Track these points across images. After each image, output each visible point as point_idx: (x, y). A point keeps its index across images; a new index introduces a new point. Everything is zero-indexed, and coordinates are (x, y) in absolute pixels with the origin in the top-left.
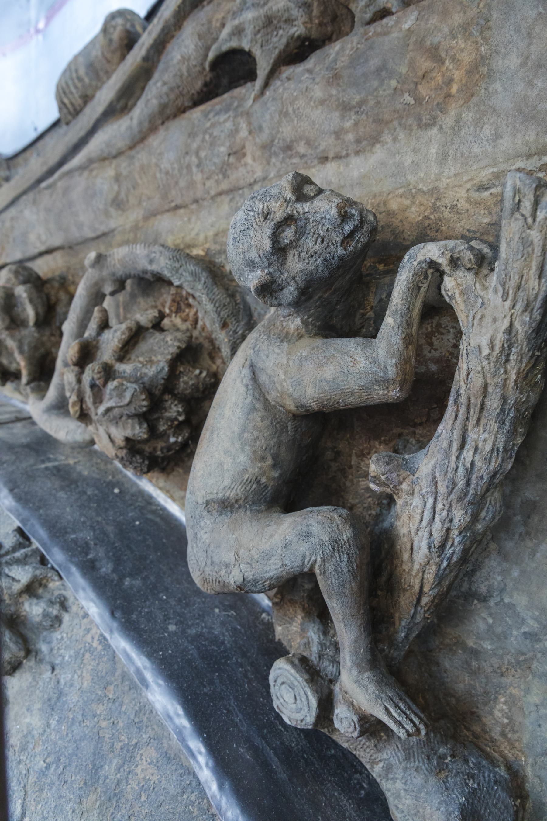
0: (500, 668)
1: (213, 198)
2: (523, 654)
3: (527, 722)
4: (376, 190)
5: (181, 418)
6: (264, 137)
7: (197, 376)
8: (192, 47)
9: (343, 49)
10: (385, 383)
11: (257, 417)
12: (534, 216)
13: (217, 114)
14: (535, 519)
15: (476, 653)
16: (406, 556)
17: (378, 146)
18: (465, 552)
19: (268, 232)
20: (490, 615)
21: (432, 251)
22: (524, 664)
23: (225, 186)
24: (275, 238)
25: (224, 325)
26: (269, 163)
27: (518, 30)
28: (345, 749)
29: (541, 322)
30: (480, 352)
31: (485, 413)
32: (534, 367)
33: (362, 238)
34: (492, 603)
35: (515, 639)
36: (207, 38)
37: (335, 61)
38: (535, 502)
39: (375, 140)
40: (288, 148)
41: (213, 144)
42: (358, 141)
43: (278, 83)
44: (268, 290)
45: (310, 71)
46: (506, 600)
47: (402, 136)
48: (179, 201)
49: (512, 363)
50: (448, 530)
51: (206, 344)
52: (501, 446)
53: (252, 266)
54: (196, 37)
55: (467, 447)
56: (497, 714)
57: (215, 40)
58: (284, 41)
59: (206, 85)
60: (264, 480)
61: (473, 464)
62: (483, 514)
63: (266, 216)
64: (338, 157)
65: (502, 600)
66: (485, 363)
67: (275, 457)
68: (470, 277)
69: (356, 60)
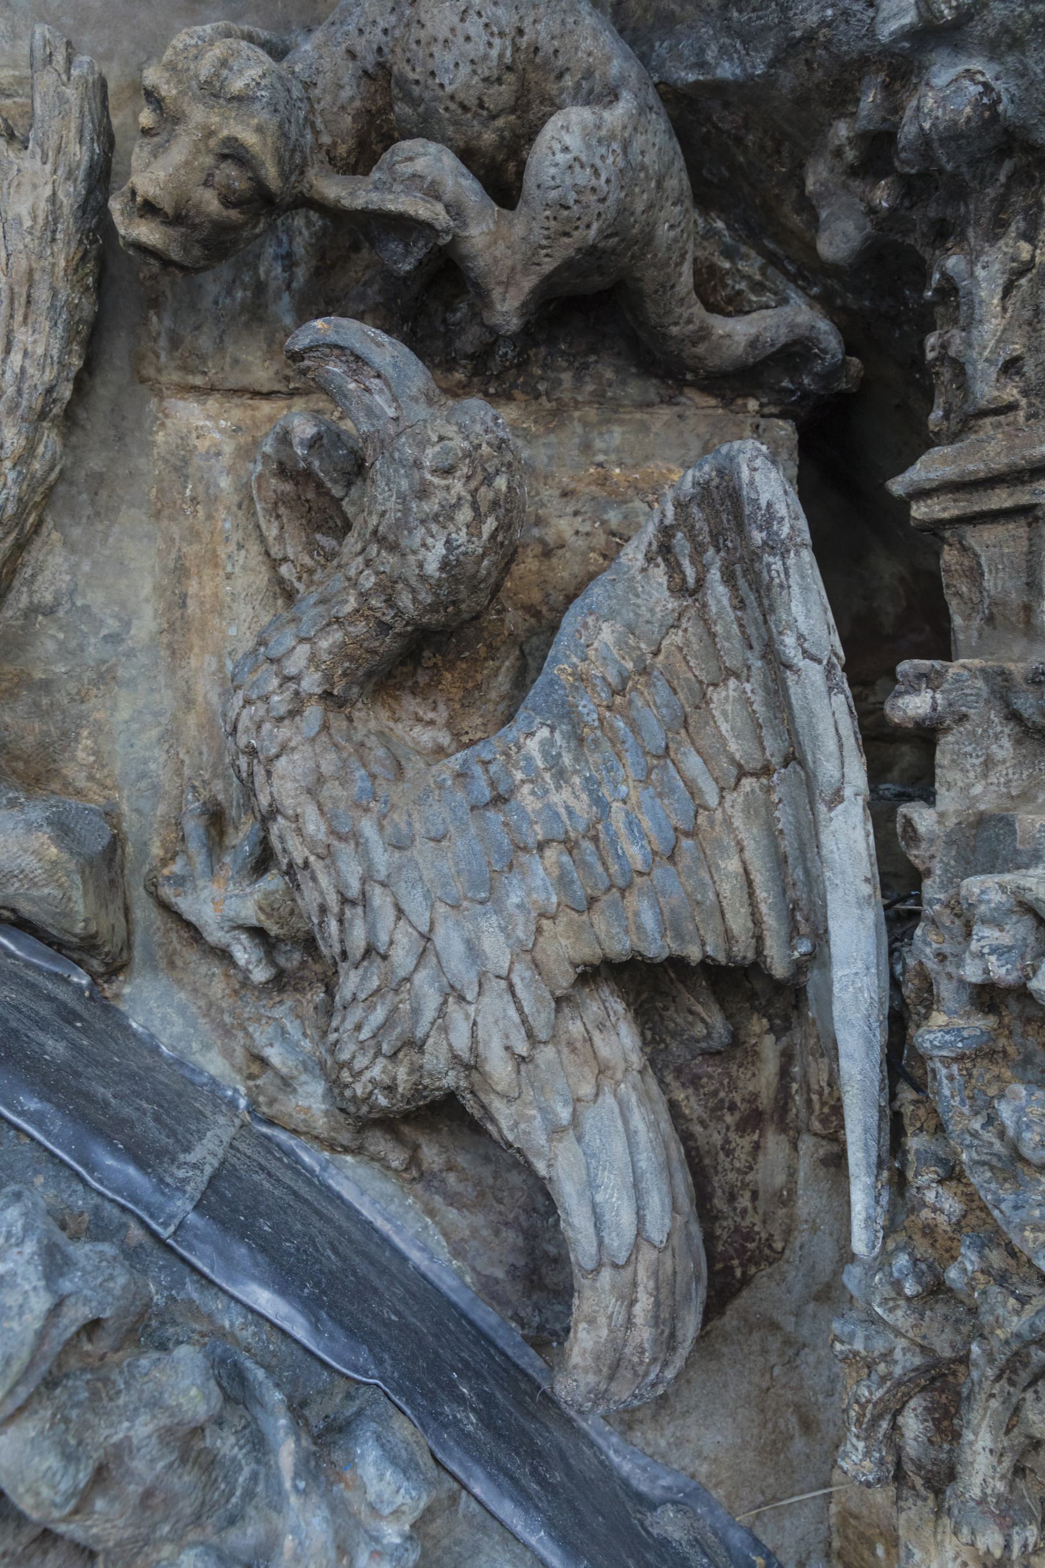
0: (78, 693)
2: (104, 662)
3: (117, 747)
12: (68, 71)
14: (104, 494)
15: (46, 686)
20: (60, 628)
22: (105, 677)
29: (86, 201)
30: (21, 224)
31: (33, 307)
32: (83, 258)
34: (61, 613)
35: (94, 649)
38: (101, 474)
46: (79, 603)
49: (59, 245)
52: (55, 353)
55: (15, 349)
56: (81, 755)
61: (23, 369)
62: (41, 449)
65: (73, 604)
66: (28, 239)
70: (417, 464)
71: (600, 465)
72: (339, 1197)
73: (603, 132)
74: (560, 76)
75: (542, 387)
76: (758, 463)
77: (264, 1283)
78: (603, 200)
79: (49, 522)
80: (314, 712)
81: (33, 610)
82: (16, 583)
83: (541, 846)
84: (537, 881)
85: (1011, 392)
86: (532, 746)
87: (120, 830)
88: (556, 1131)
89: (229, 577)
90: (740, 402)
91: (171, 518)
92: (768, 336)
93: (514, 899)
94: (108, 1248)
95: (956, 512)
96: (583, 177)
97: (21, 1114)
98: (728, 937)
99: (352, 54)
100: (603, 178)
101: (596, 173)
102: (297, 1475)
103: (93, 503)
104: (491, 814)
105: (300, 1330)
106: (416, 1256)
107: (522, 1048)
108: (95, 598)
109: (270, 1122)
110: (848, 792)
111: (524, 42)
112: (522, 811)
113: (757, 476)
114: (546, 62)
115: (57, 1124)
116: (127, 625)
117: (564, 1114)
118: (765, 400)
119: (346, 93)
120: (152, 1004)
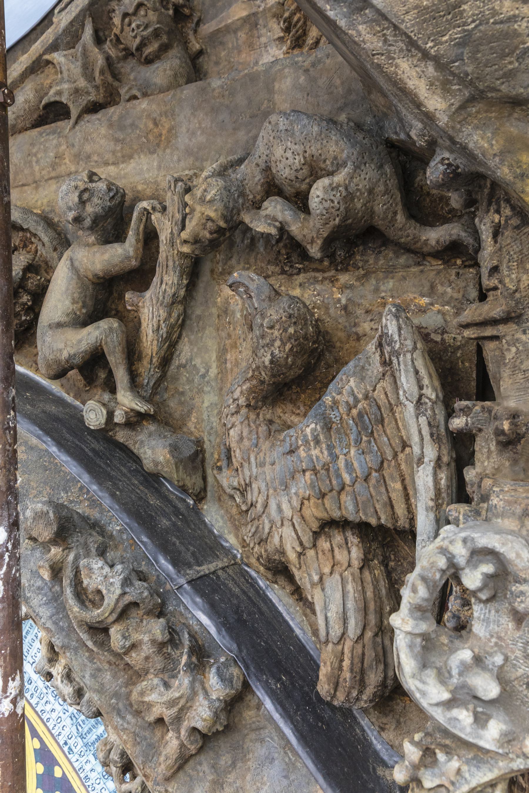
1: (46, 181)
4: (132, 180)
5: (29, 304)
6: (76, 150)
7: (39, 280)
10: (128, 258)
11: (74, 282)
13: (47, 135)
14: (201, 322)
15: (183, 393)
16: (144, 340)
17: (132, 160)
18: (169, 334)
19: (77, 194)
21: (144, 204)
23: (53, 174)
24: (80, 197)
25: (55, 250)
26: (78, 164)
27: (185, 117)
33: (118, 199)
36: (41, 92)
37: (111, 117)
39: (131, 157)
40: (88, 157)
41: (46, 151)
42: (123, 157)
43: (83, 123)
44: (78, 220)
45: (99, 120)
47: (142, 157)
50: (159, 321)
51: (43, 265)
52: (176, 282)
53: (70, 209)
54: (34, 91)
56: (193, 419)
57: (47, 94)
58: (85, 102)
60: (78, 313)
63: (76, 188)
64: (114, 164)
67: (84, 302)
69: (121, 117)
70: (262, 325)
71: (383, 298)
72: (271, 601)
73: (335, 185)
74: (325, 161)
75: (360, 264)
76: (389, 317)
77: (204, 612)
78: (339, 210)
79: (184, 334)
80: (244, 411)
82: (174, 357)
83: (304, 471)
84: (302, 485)
86: (308, 430)
87: (202, 447)
88: (313, 585)
89: (240, 352)
90: (453, 261)
91: (222, 330)
92: (442, 239)
93: (293, 491)
94: (145, 584)
95: (476, 335)
96: (327, 204)
97: (142, 542)
98: (394, 517)
99: (258, 165)
100: (336, 202)
101: (332, 201)
102: (185, 665)
104: (289, 457)
105: (213, 630)
106: (298, 631)
107: (299, 549)
108: (197, 361)
109: (247, 565)
110: (426, 460)
111: (307, 155)
112: (299, 457)
113: (388, 322)
115: (150, 546)
116: (208, 371)
117: (316, 578)
118: (464, 259)
119: (257, 179)
120: (213, 514)
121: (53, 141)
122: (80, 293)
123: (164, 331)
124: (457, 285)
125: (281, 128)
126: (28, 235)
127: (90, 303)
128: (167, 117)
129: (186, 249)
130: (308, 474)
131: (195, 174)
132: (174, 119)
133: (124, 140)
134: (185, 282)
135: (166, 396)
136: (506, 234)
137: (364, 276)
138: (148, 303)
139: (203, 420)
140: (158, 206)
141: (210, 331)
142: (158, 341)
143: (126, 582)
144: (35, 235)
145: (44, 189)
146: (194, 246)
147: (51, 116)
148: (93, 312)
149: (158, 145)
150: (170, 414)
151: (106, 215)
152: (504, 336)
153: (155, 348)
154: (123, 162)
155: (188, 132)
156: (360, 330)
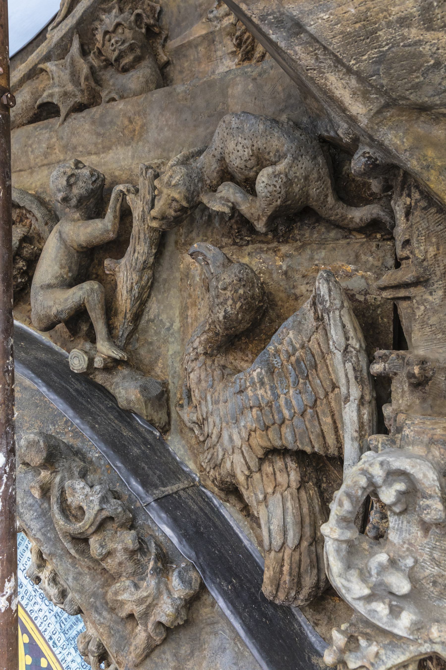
4: (110, 167)
5: (25, 268)
6: (64, 142)
7: (33, 249)
8: (28, 97)
9: (97, 111)
10: (107, 231)
11: (62, 251)
14: (167, 285)
15: (151, 343)
16: (120, 299)
17: (111, 151)
18: (140, 294)
19: (65, 179)
21: (121, 187)
23: (45, 162)
24: (68, 181)
25: (46, 224)
26: (66, 153)
27: (155, 116)
28: (101, 385)
33: (99, 182)
36: (36, 95)
37: (94, 115)
39: (110, 148)
40: (75, 148)
41: (39, 142)
42: (103, 148)
44: (66, 200)
48: (21, 168)
50: (132, 283)
51: (36, 236)
52: (146, 251)
53: (59, 191)
56: (159, 364)
57: (41, 96)
58: (72, 103)
59: (35, 114)
60: (65, 276)
63: (65, 173)
64: (95, 154)
67: (70, 268)
68: (133, 196)
69: (102, 116)
70: (217, 287)
71: (316, 265)
72: (224, 517)
74: (269, 153)
75: (298, 237)
76: (321, 281)
77: (168, 526)
78: (280, 193)
79: (153, 294)
80: (202, 358)
81: (149, 321)
83: (251, 408)
84: (250, 419)
85: (406, 253)
86: (255, 374)
87: (167, 388)
88: (259, 502)
90: (374, 235)
91: (185, 291)
92: (364, 218)
93: (242, 424)
94: (119, 502)
95: (392, 296)
96: (271, 189)
97: (116, 466)
98: (325, 445)
99: (214, 156)
100: (278, 187)
101: (275, 186)
102: (152, 570)
103: (164, 287)
104: (239, 396)
106: (246, 542)
107: (247, 473)
108: (164, 317)
109: (204, 487)
110: (352, 398)
111: (254, 148)
112: (247, 396)
114: (263, 151)
115: (124, 470)
116: (172, 325)
117: (261, 497)
118: (383, 233)
119: (213, 167)
121: (46, 134)
122: (67, 260)
123: (136, 291)
124: (377, 255)
125: (233, 126)
126: (24, 212)
127: (75, 268)
128: (139, 115)
129: (155, 224)
130: (254, 410)
131: (163, 163)
132: (145, 118)
133: (104, 134)
134: (154, 251)
135: (137, 345)
136: (416, 214)
137: (301, 247)
138: (123, 268)
139: (168, 366)
140: (132, 189)
141: (174, 292)
142: (131, 300)
143: (103, 500)
144: (30, 212)
145: (38, 174)
146: (161, 222)
147: (44, 114)
148: (78, 275)
149: (132, 139)
150: (141, 361)
151: (89, 196)
152: (415, 297)
153: (129, 306)
154: (103, 152)
155: (157, 128)
156: (298, 292)
